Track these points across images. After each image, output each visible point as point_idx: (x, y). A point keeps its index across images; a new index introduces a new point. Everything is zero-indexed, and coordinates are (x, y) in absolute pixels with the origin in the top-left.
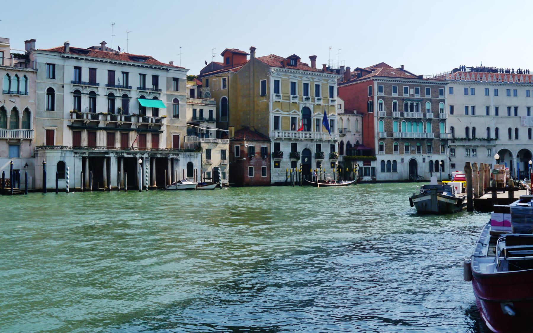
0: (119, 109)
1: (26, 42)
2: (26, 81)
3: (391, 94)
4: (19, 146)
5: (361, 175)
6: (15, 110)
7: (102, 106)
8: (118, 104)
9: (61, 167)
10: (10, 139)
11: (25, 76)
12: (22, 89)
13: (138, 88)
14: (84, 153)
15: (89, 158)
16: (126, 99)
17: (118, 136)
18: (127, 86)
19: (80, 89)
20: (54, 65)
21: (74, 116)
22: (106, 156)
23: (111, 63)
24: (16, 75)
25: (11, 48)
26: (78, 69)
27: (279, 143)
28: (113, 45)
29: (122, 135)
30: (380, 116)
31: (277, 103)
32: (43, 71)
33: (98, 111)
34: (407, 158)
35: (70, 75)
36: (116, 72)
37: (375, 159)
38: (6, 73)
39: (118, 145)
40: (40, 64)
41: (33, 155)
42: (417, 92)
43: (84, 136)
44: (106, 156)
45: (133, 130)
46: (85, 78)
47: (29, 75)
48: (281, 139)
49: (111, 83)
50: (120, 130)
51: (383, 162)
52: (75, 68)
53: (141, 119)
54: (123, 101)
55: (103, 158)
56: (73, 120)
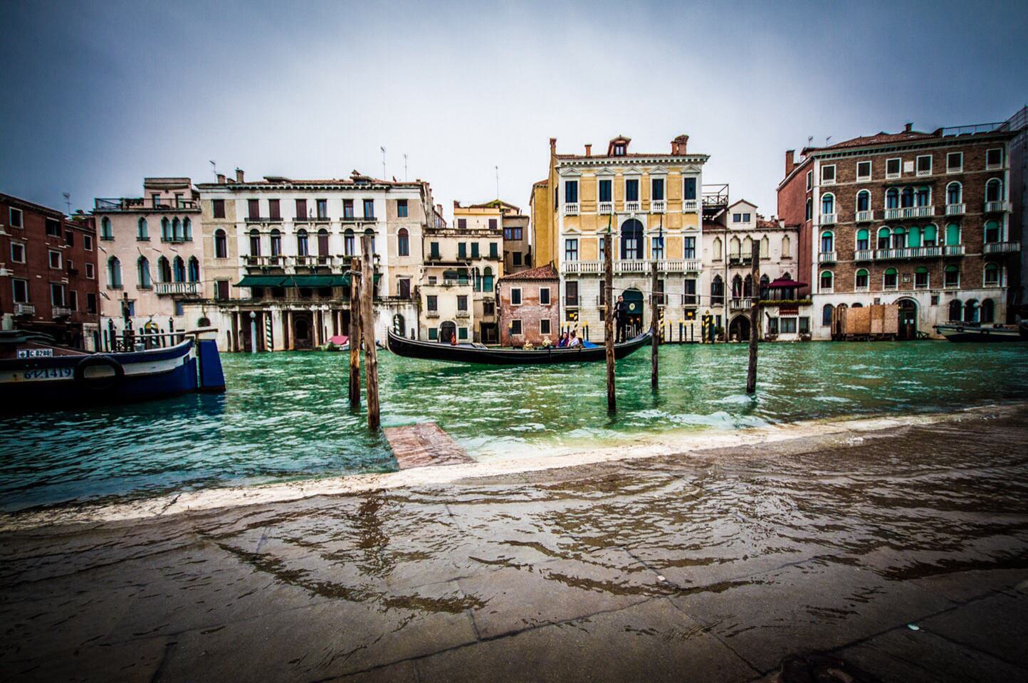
3: (855, 179)
5: (773, 331)
6: (179, 261)
7: (289, 246)
22: (265, 309)
27: (577, 282)
30: (822, 223)
31: (571, 218)
32: (208, 210)
34: (889, 298)
36: (281, 202)
37: (809, 304)
42: (924, 165)
44: (265, 309)
46: (264, 212)
48: (577, 274)
49: (301, 216)
51: (828, 308)
54: (319, 237)
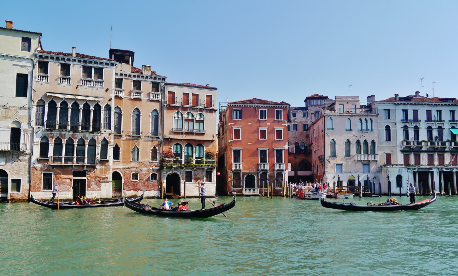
0: (436, 137)
1: (368, 97)
2: (371, 123)
4: (369, 165)
6: (366, 142)
7: (423, 136)
8: (435, 133)
9: (399, 178)
10: (364, 161)
11: (371, 119)
12: (369, 128)
13: (449, 121)
14: (415, 169)
15: (419, 173)
16: (440, 129)
17: (436, 156)
18: (440, 120)
19: (407, 125)
20: (389, 110)
21: (405, 143)
22: (430, 170)
23: (428, 104)
24: (366, 119)
25: (360, 102)
26: (406, 111)
28: (423, 94)
29: (439, 155)
32: (383, 114)
33: (421, 139)
35: (400, 116)
38: (359, 118)
39: (436, 162)
40: (380, 110)
41: (378, 171)
43: (412, 157)
44: (430, 170)
45: (447, 152)
46: (411, 116)
47: (373, 118)
49: (429, 119)
50: (438, 152)
52: (403, 110)
53: (453, 144)
54: (438, 131)
55: (428, 172)
56: (403, 147)
